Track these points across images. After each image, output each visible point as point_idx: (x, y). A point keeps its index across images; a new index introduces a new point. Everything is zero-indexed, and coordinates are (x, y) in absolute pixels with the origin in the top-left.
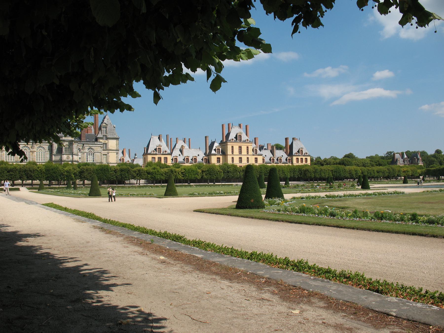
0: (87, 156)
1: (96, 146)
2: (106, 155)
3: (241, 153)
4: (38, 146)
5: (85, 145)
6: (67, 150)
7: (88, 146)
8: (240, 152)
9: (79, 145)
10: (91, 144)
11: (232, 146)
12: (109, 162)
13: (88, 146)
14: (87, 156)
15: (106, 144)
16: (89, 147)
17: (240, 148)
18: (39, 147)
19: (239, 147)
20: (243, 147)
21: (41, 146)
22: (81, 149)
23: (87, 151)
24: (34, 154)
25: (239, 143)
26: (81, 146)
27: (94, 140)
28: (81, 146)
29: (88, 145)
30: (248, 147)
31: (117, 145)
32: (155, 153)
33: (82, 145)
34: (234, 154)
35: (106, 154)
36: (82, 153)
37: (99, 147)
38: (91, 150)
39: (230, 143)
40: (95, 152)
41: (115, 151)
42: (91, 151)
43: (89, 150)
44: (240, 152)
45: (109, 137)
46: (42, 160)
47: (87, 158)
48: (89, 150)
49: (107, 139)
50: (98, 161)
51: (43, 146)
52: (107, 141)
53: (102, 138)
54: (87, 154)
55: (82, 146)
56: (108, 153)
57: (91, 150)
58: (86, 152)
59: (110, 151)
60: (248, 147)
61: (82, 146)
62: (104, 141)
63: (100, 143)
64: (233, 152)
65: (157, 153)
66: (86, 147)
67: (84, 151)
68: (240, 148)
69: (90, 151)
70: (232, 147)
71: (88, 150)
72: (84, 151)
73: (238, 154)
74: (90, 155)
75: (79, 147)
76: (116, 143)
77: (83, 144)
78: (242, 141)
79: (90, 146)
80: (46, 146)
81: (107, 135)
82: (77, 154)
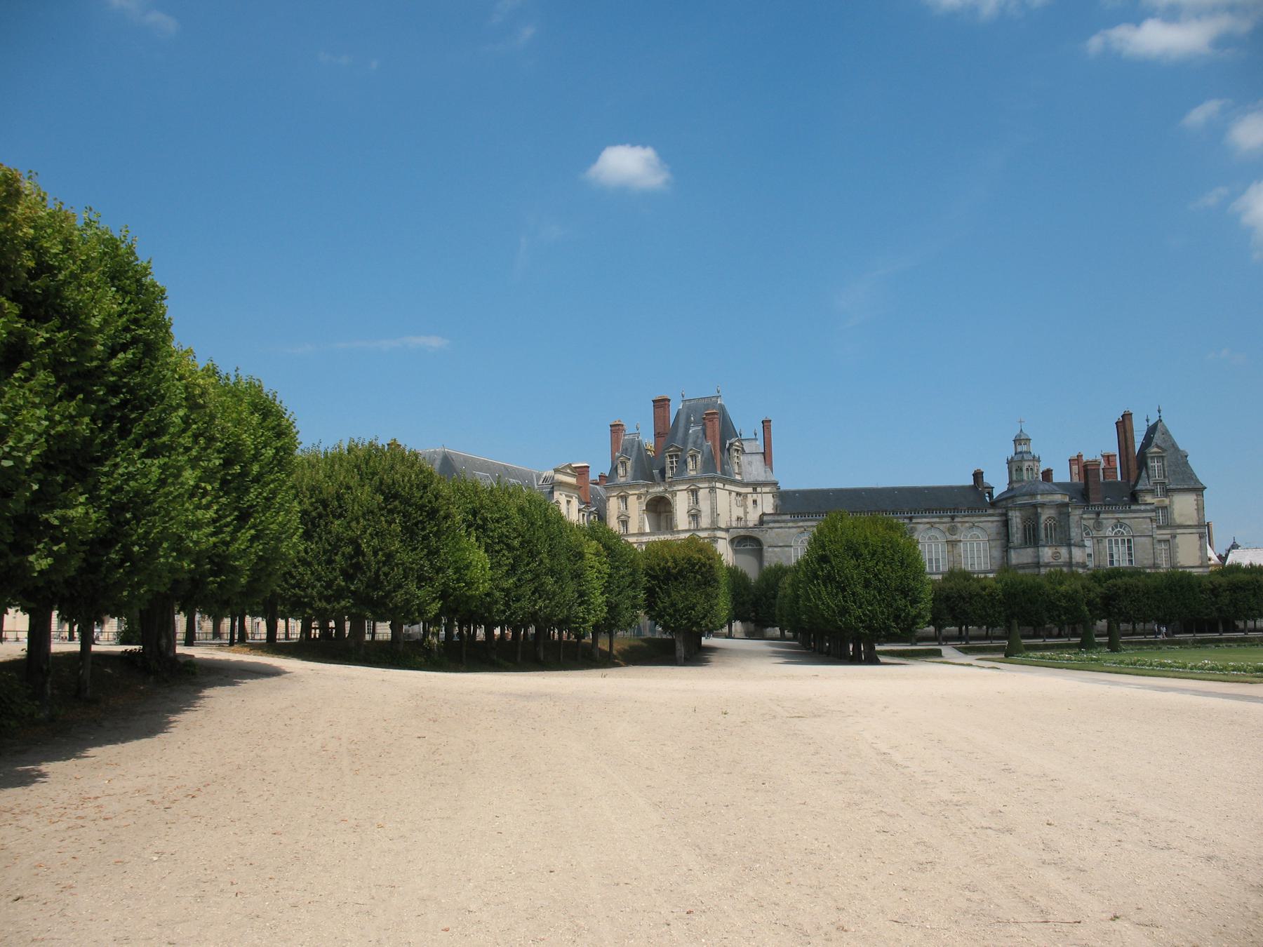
0: (1111, 548)
4: (967, 525)
5: (1102, 516)
6: (1051, 536)
7: (1113, 518)
9: (1085, 516)
12: (1178, 565)
13: (1113, 518)
14: (1111, 548)
16: (1114, 521)
22: (1092, 528)
23: (1109, 532)
24: (957, 547)
26: (1090, 519)
27: (1125, 499)
28: (1090, 519)
29: (1110, 516)
33: (1093, 516)
35: (1169, 541)
36: (1095, 540)
37: (1143, 518)
38: (1122, 530)
40: (1133, 536)
41: (1194, 531)
42: (1123, 533)
43: (1116, 530)
46: (979, 564)
47: (1112, 556)
48: (1116, 530)
50: (1145, 562)
51: (981, 524)
52: (1167, 501)
53: (1152, 491)
54: (1110, 541)
55: (1093, 519)
56: (1174, 536)
57: (1122, 530)
58: (1106, 537)
59: (1179, 531)
61: (1093, 519)
62: (1160, 501)
63: (1148, 507)
66: (1105, 521)
67: (1101, 534)
69: (1119, 531)
71: (1113, 529)
72: (1101, 534)
74: (1120, 545)
75: (1084, 522)
77: (1098, 514)
79: (1117, 518)
80: (990, 524)
81: (1167, 481)
82: (1081, 543)
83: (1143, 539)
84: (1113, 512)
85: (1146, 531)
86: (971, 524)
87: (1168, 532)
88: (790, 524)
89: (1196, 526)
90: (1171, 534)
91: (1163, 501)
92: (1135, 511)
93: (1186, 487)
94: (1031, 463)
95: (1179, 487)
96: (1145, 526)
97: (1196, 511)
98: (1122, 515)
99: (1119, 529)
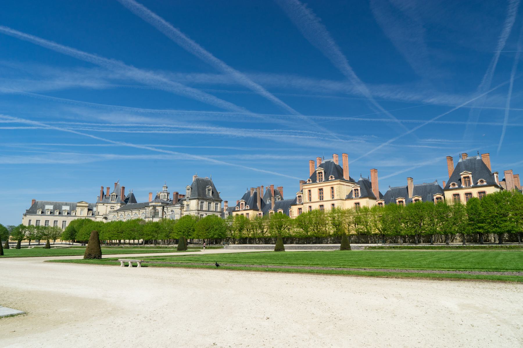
3: (323, 199)
5: (168, 208)
8: (321, 198)
10: (172, 207)
11: (309, 189)
15: (189, 205)
17: (321, 190)
18: (143, 213)
19: (320, 189)
20: (324, 188)
23: (171, 213)
25: (318, 184)
30: (332, 188)
31: (196, 205)
32: (238, 209)
34: (312, 201)
39: (307, 185)
41: (194, 212)
44: (321, 198)
49: (190, 199)
53: (185, 200)
54: (170, 216)
57: (173, 212)
60: (332, 188)
62: (187, 203)
64: (310, 199)
66: (169, 210)
67: (168, 214)
68: (321, 190)
70: (310, 191)
73: (318, 200)
77: (167, 208)
78: (324, 180)
79: (171, 209)
84: (171, 207)
87: (188, 212)
88: (112, 214)
89: (195, 210)
93: (193, 198)
95: (191, 198)
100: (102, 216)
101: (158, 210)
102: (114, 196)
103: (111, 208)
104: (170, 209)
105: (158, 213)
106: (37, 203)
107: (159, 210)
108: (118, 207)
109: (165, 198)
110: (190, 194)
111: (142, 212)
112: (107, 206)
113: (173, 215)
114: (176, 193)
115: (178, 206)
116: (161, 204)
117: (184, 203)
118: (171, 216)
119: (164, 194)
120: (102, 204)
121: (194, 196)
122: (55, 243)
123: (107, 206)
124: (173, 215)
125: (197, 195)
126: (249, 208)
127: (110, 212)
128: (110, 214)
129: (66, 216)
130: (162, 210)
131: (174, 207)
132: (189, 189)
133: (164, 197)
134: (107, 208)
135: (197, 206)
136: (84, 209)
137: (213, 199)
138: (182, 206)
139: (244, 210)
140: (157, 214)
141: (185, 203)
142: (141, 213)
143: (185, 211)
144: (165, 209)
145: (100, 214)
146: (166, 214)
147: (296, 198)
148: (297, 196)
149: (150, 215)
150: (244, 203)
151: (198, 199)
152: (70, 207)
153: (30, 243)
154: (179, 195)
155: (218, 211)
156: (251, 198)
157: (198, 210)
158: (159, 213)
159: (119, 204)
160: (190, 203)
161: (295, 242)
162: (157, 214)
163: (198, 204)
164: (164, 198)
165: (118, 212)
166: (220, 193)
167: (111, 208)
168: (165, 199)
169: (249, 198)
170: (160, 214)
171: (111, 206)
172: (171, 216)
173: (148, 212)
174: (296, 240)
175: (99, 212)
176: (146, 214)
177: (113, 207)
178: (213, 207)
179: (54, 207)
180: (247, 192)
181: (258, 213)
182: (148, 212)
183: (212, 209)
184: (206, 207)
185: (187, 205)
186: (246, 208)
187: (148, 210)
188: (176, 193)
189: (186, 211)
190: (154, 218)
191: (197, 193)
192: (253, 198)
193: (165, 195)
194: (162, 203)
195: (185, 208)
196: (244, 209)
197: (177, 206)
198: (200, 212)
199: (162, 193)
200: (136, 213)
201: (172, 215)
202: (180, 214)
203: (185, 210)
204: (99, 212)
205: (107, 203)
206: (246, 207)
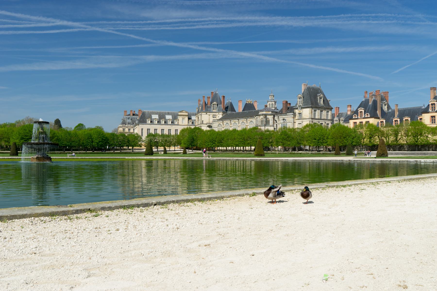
1: (288, 117)
2: (301, 124)
5: (279, 117)
10: (284, 116)
15: (301, 113)
18: (251, 121)
21: (252, 121)
23: (282, 121)
26: (277, 118)
32: (356, 117)
41: (308, 120)
42: (285, 122)
45: (303, 107)
48: (283, 121)
49: (302, 108)
53: (297, 109)
54: (282, 124)
56: (302, 122)
57: (285, 121)
59: (304, 120)
62: (299, 111)
65: (359, 117)
67: (279, 122)
69: (284, 121)
76: (309, 112)
77: (278, 117)
79: (283, 118)
83: (289, 123)
84: (282, 116)
85: (291, 121)
86: (251, 121)
87: (301, 121)
88: (217, 122)
89: (308, 119)
90: (302, 121)
91: (300, 111)
92: (288, 115)
93: (306, 106)
94: (270, 102)
95: (304, 107)
96: (290, 120)
97: (309, 114)
98: (284, 116)
99: (284, 121)
100: (206, 124)
101: (268, 118)
102: (215, 105)
103: (213, 117)
104: (281, 117)
105: (269, 121)
106: (145, 113)
107: (270, 118)
108: (220, 115)
109: (273, 106)
110: (302, 103)
111: (250, 121)
112: (209, 115)
113: (285, 124)
114: (285, 102)
115: (291, 115)
116: (271, 112)
117: (296, 112)
118: (283, 124)
119: (272, 102)
120: (205, 114)
121: (307, 105)
122: (175, 150)
123: (209, 115)
124: (285, 124)
125: (310, 103)
126: (369, 116)
127: (214, 121)
128: (214, 122)
129: (170, 125)
130: (273, 119)
131: (286, 115)
132: (301, 98)
133: (272, 105)
134: (209, 117)
135: (311, 114)
136: (185, 118)
137: (325, 107)
138: (295, 115)
139: (364, 118)
140: (268, 123)
141: (297, 111)
142: (249, 122)
143: (297, 120)
144: (275, 117)
145: (204, 123)
146: (277, 122)
147: (429, 105)
148: (430, 103)
149: (260, 123)
150: (363, 111)
151: (312, 107)
152: (172, 116)
153: (157, 150)
154: (288, 104)
155: (329, 119)
156: (370, 106)
157: (312, 119)
158: (270, 121)
159: (221, 113)
160: (303, 111)
161: (431, 150)
162: (268, 123)
163: (311, 113)
164: (272, 106)
165: (223, 121)
166: (330, 100)
167: (213, 117)
168: (273, 108)
169: (368, 106)
170: (271, 122)
171: (213, 115)
172: (283, 124)
173: (259, 120)
174: (433, 148)
175: (203, 121)
176: (258, 123)
177: (215, 116)
178: (324, 115)
179: (159, 116)
180: (364, 100)
181: (380, 121)
182: (259, 121)
183: (324, 117)
184: (318, 115)
185: (299, 114)
186: (366, 116)
187: (259, 118)
188: (285, 102)
189: (298, 119)
190: (266, 127)
191: (310, 102)
192: (372, 106)
193: (273, 104)
194: (272, 112)
195: (297, 116)
196: (363, 117)
197: (289, 115)
198: (314, 120)
199: (270, 102)
200: (244, 121)
201: (284, 123)
202: (293, 122)
203: (297, 118)
204: (203, 121)
205: (210, 112)
206: (366, 115)
